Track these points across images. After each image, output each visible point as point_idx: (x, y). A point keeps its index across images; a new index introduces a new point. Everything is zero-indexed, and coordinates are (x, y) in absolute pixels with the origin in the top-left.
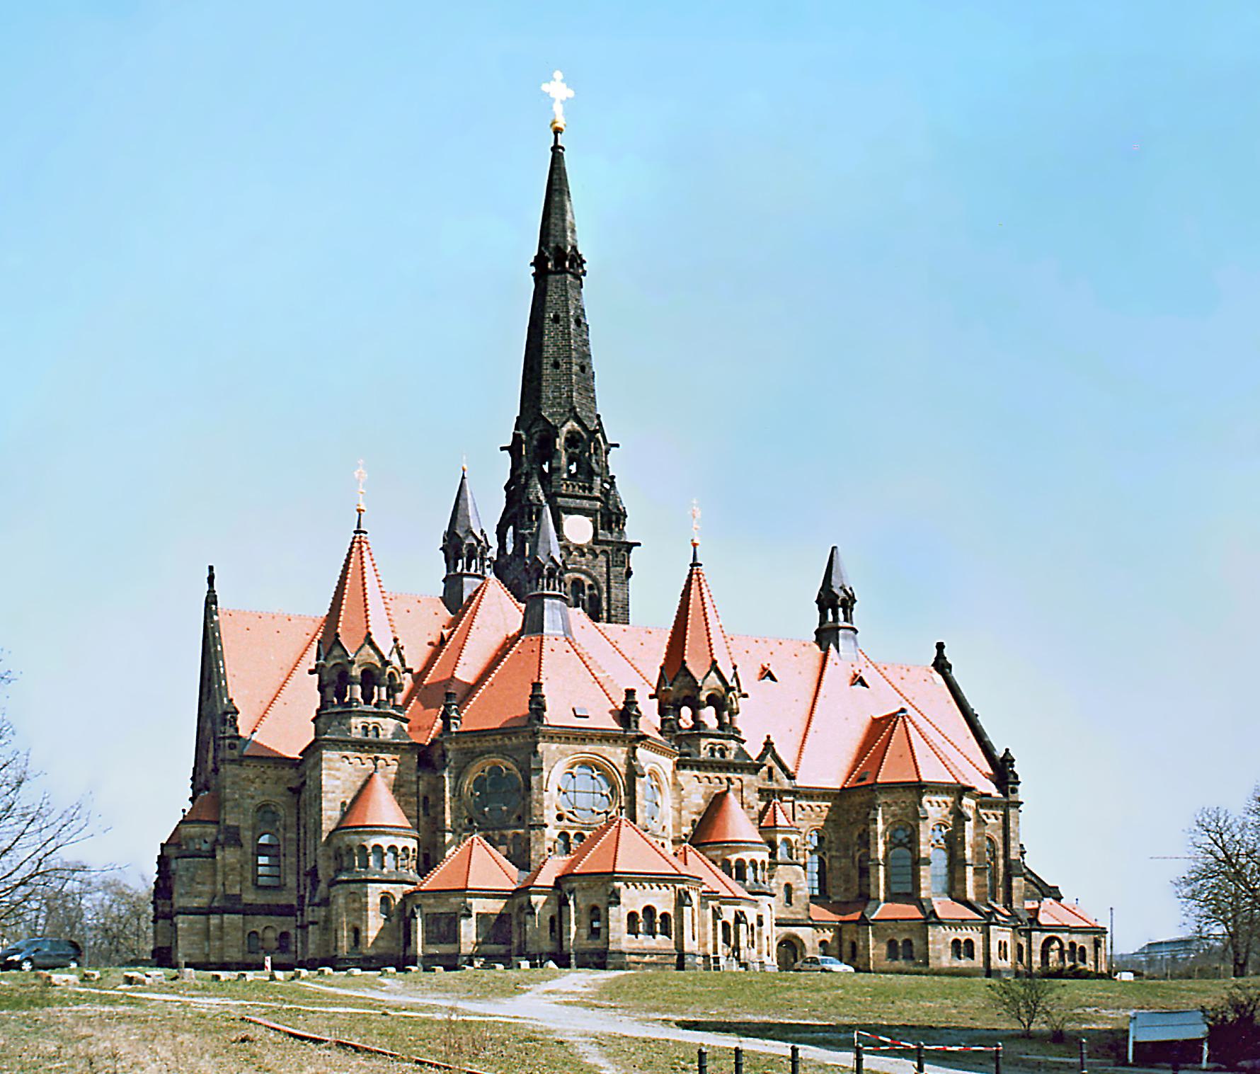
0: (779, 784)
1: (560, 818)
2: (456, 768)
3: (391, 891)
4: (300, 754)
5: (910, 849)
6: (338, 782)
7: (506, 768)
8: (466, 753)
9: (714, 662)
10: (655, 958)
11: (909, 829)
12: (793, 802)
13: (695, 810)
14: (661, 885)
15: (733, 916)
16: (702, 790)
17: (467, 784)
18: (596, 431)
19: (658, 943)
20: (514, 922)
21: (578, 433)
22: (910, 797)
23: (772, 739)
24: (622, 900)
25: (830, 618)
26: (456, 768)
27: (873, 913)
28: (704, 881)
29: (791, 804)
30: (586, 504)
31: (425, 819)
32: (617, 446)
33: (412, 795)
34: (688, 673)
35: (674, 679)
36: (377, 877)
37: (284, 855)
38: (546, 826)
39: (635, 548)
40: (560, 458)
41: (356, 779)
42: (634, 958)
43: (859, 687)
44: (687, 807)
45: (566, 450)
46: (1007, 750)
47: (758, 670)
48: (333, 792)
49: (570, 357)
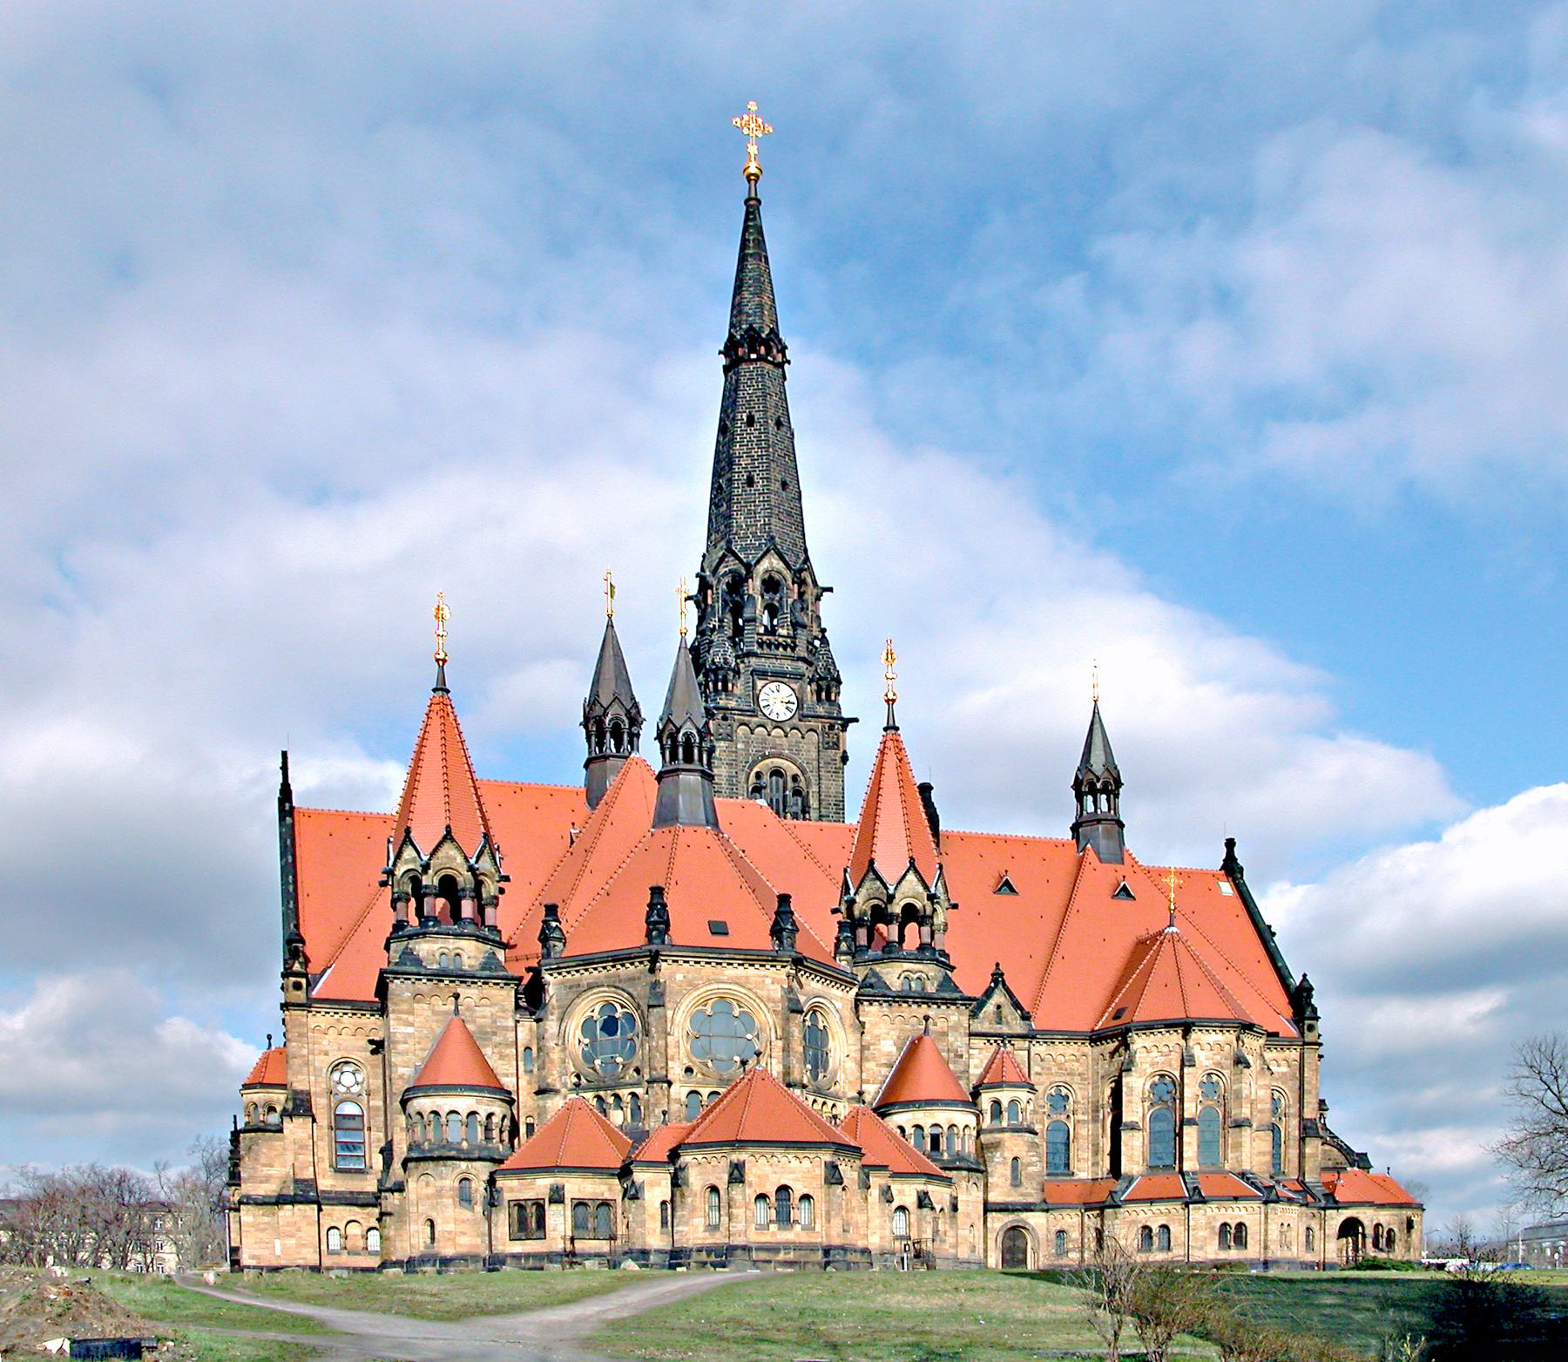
0: (1010, 1028)
1: (689, 1070)
2: (559, 1007)
3: (473, 1171)
4: (376, 996)
6: (410, 1030)
7: (622, 1007)
8: (571, 987)
10: (791, 1256)
13: (884, 1061)
14: (801, 1156)
15: (914, 1199)
16: (894, 1034)
17: (574, 1026)
18: (801, 571)
19: (797, 1235)
20: (619, 1211)
22: (1175, 1038)
24: (750, 1176)
25: (1090, 808)
26: (559, 1007)
27: (1124, 1192)
28: (863, 1151)
30: (788, 666)
31: (527, 1077)
32: (830, 590)
33: (508, 1045)
34: (878, 878)
35: (860, 886)
36: (453, 1153)
37: (369, 1129)
38: (670, 1084)
39: (851, 725)
40: (755, 607)
41: (434, 1025)
42: (763, 1256)
44: (874, 1059)
45: (763, 597)
46: (1305, 976)
47: (992, 882)
48: (406, 1043)
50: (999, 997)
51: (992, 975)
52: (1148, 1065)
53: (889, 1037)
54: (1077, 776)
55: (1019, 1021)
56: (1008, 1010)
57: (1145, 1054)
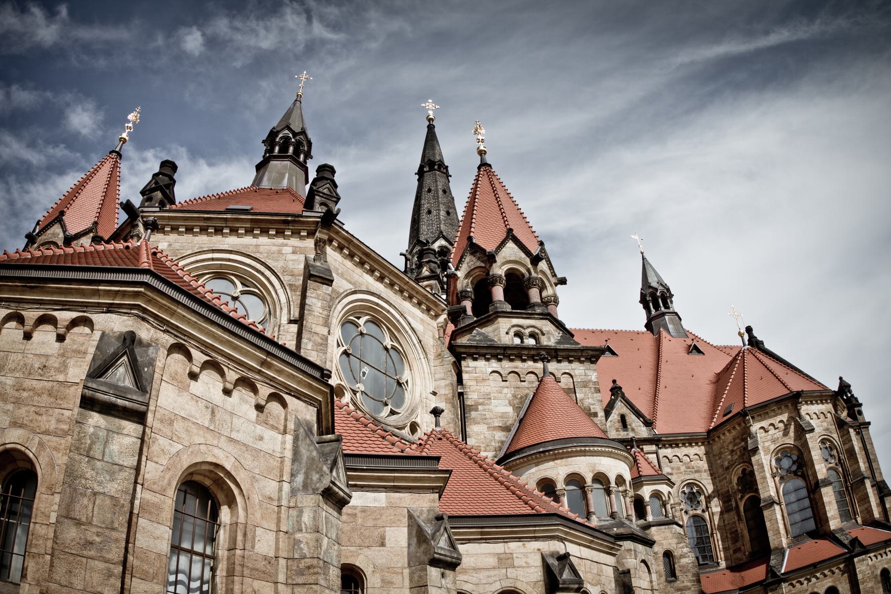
5: (804, 477)
9: (510, 231)
11: (796, 452)
12: (656, 453)
21: (446, 247)
23: (619, 383)
29: (655, 455)
43: (696, 357)
49: (438, 206)
50: (620, 408)
51: (611, 390)
52: (769, 443)
53: (502, 396)
54: (641, 293)
55: (644, 429)
56: (631, 418)
57: (764, 434)
